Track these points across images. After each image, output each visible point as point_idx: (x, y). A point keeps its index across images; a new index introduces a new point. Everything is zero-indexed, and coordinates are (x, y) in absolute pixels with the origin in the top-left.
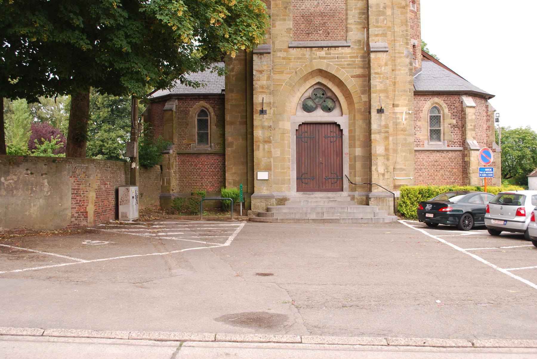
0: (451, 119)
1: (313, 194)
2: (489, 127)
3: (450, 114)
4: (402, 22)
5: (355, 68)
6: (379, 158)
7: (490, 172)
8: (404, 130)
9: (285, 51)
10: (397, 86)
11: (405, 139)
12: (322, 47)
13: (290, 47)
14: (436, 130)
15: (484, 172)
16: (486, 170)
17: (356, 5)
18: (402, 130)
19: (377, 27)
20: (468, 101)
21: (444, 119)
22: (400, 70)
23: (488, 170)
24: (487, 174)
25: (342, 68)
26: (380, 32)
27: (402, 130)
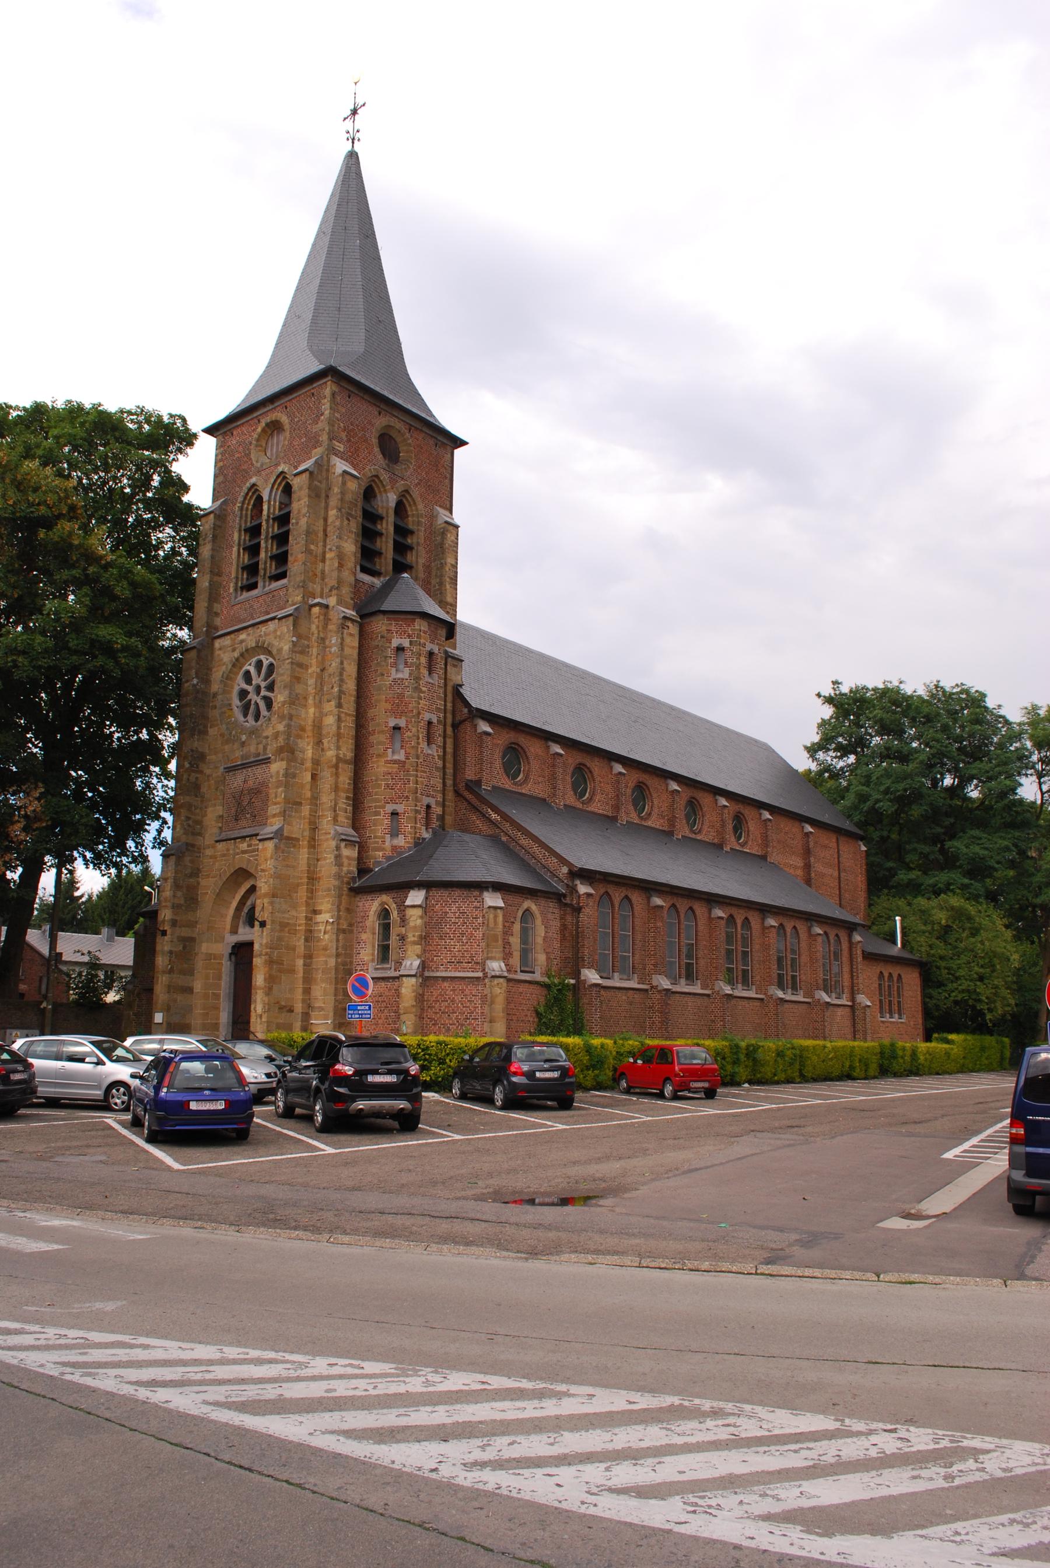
8: (325, 949)
9: (213, 847)
12: (244, 837)
13: (217, 841)
15: (356, 1012)
16: (359, 1008)
18: (323, 949)
23: (363, 1007)
26: (278, 811)
27: (323, 949)
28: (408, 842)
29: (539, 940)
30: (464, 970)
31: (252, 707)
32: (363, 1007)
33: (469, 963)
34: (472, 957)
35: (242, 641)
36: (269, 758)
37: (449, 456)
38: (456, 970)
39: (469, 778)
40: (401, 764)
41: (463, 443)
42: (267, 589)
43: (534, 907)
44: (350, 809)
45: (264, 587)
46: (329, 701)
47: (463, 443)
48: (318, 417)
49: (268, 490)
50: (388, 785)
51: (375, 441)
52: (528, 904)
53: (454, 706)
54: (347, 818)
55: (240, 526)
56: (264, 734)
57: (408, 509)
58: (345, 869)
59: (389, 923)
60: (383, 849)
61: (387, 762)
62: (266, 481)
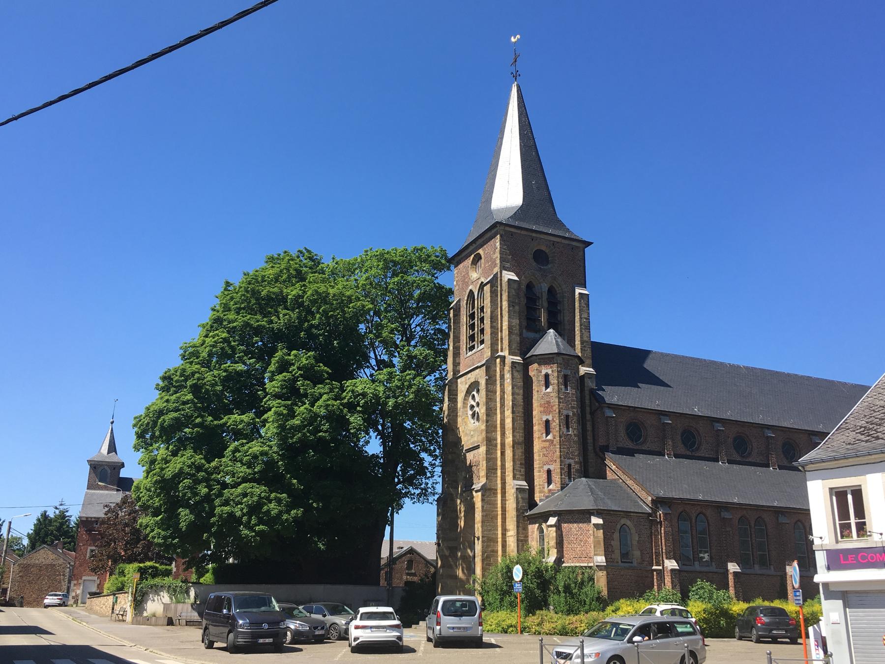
28: (557, 487)
29: (635, 543)
30: (583, 562)
31: (476, 415)
33: (586, 557)
34: (587, 554)
35: (469, 379)
37: (582, 252)
38: (578, 562)
39: (602, 444)
40: (551, 441)
41: (590, 244)
42: (479, 349)
43: (628, 523)
44: (523, 470)
45: (478, 347)
46: (508, 410)
47: (590, 244)
48: (495, 250)
49: (477, 292)
50: (544, 454)
51: (531, 256)
52: (623, 521)
53: (591, 402)
54: (521, 475)
55: (467, 314)
57: (557, 289)
58: (520, 505)
59: (543, 535)
61: (545, 441)
62: (476, 288)
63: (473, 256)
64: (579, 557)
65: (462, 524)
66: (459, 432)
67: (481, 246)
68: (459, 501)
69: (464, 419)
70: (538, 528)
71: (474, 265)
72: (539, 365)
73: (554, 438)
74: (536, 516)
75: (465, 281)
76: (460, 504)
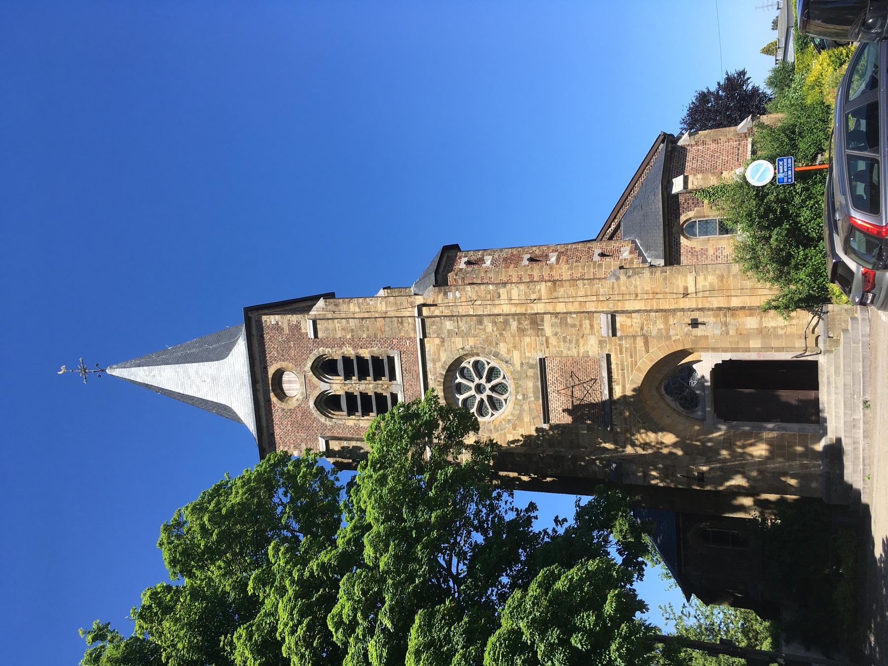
0: (703, 206)
1: (823, 403)
2: (714, 141)
3: (696, 208)
4: (573, 286)
5: (635, 348)
6: (764, 325)
7: (785, 164)
8: (721, 278)
10: (658, 290)
11: (735, 276)
14: (719, 225)
17: (555, 346)
18: (722, 281)
19: (581, 326)
20: (678, 185)
21: (704, 217)
22: (635, 287)
24: (788, 170)
25: (636, 365)
26: (587, 322)
27: (722, 281)
32: (781, 167)
36: (540, 359)
56: (519, 369)
60: (632, 259)
62: (315, 387)
63: (272, 394)
64: (738, 155)
65: (669, 438)
66: (513, 442)
67: (265, 369)
68: (629, 450)
69: (495, 426)
70: (687, 238)
71: (285, 398)
72: (451, 272)
73: (556, 251)
74: (667, 238)
75: (300, 420)
76: (633, 445)
